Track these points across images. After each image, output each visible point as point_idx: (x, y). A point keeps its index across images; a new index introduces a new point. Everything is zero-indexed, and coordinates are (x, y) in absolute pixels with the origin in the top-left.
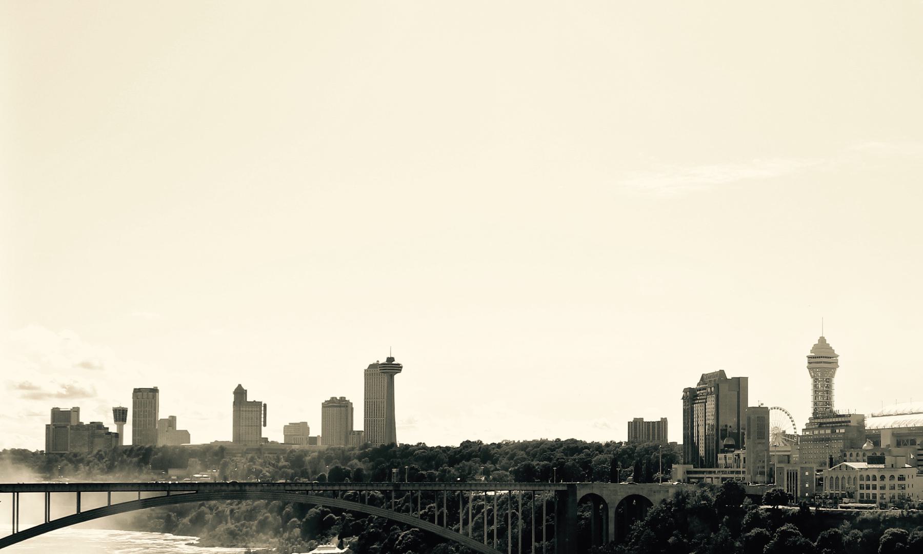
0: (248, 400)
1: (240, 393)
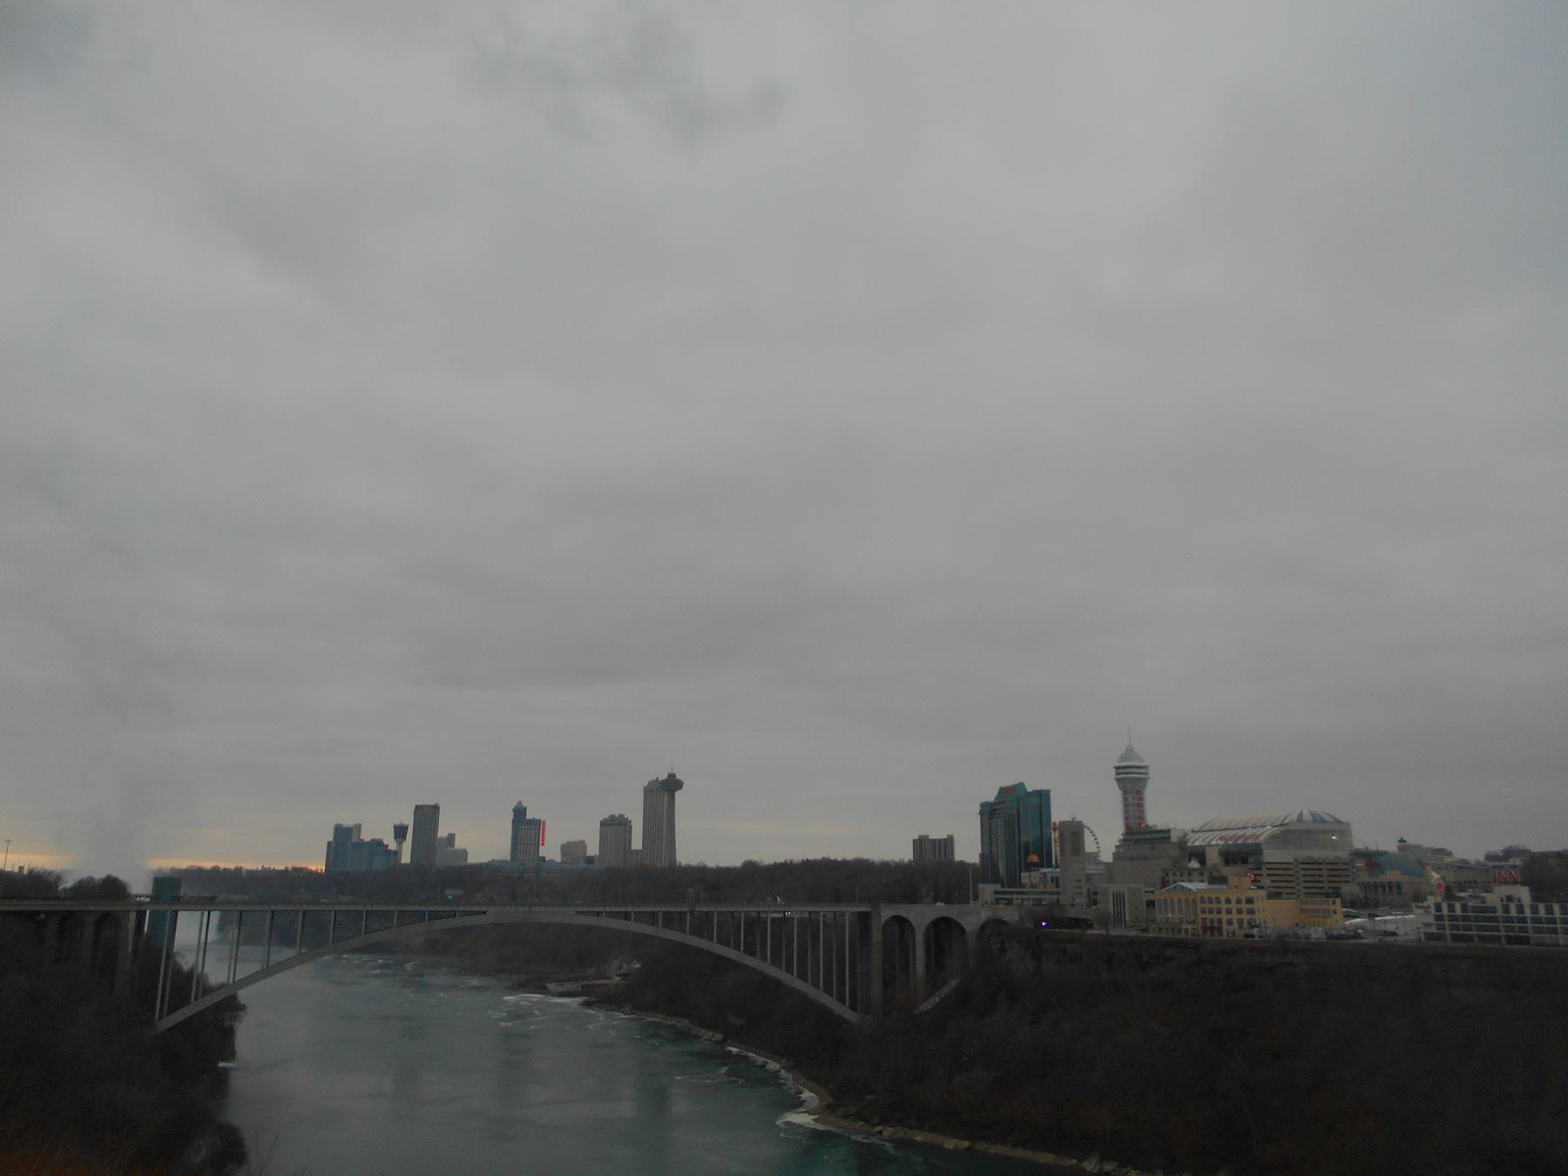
1: (519, 812)
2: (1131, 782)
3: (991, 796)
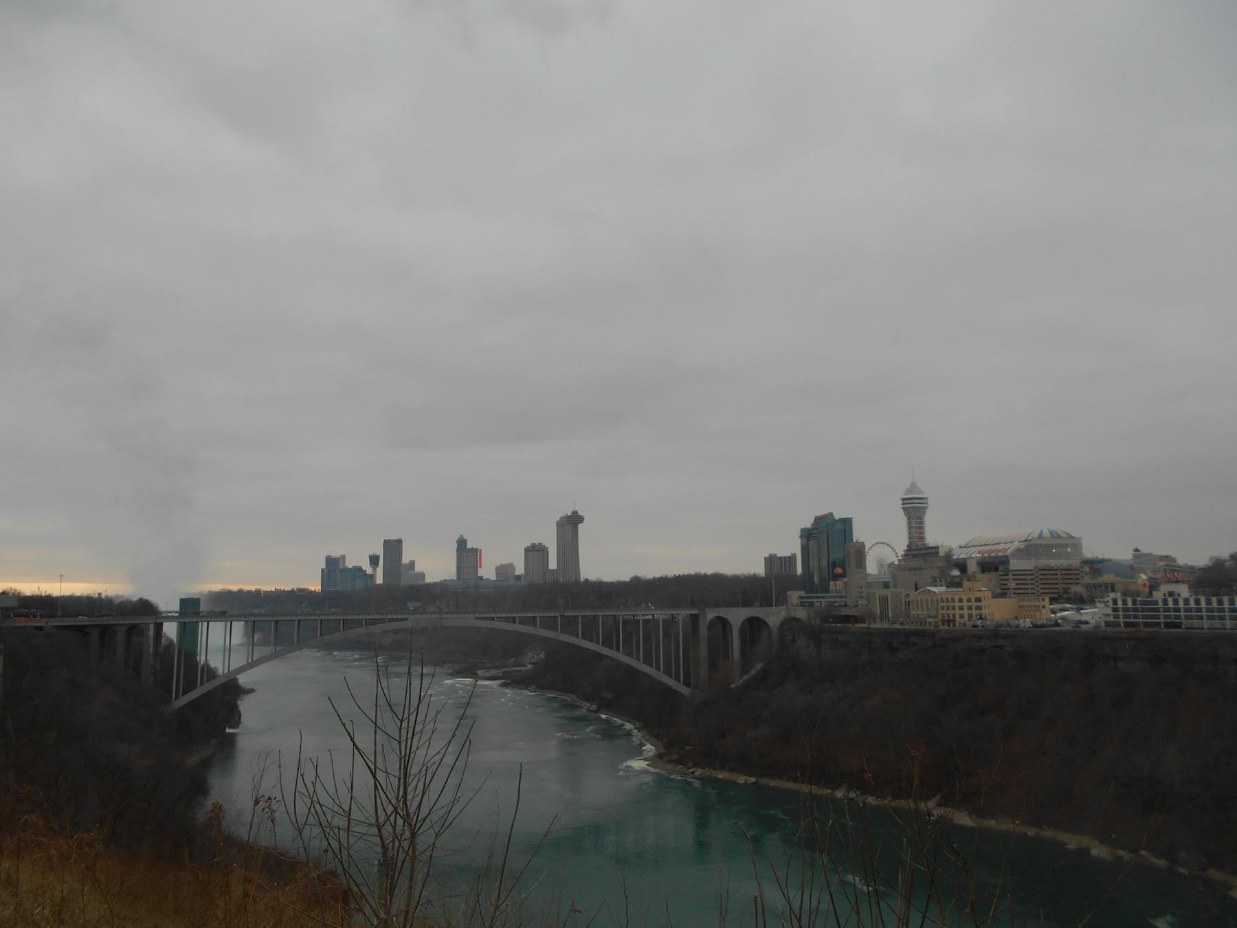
0: (468, 547)
1: (462, 543)
2: (914, 510)
3: (808, 524)
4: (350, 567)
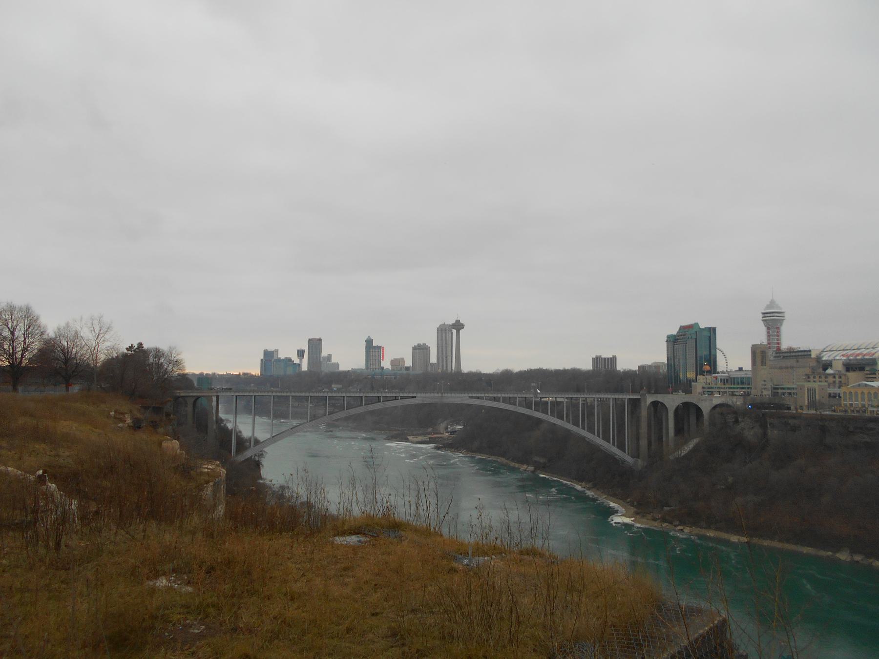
1: (369, 342)
3: (674, 331)
4: (283, 358)
